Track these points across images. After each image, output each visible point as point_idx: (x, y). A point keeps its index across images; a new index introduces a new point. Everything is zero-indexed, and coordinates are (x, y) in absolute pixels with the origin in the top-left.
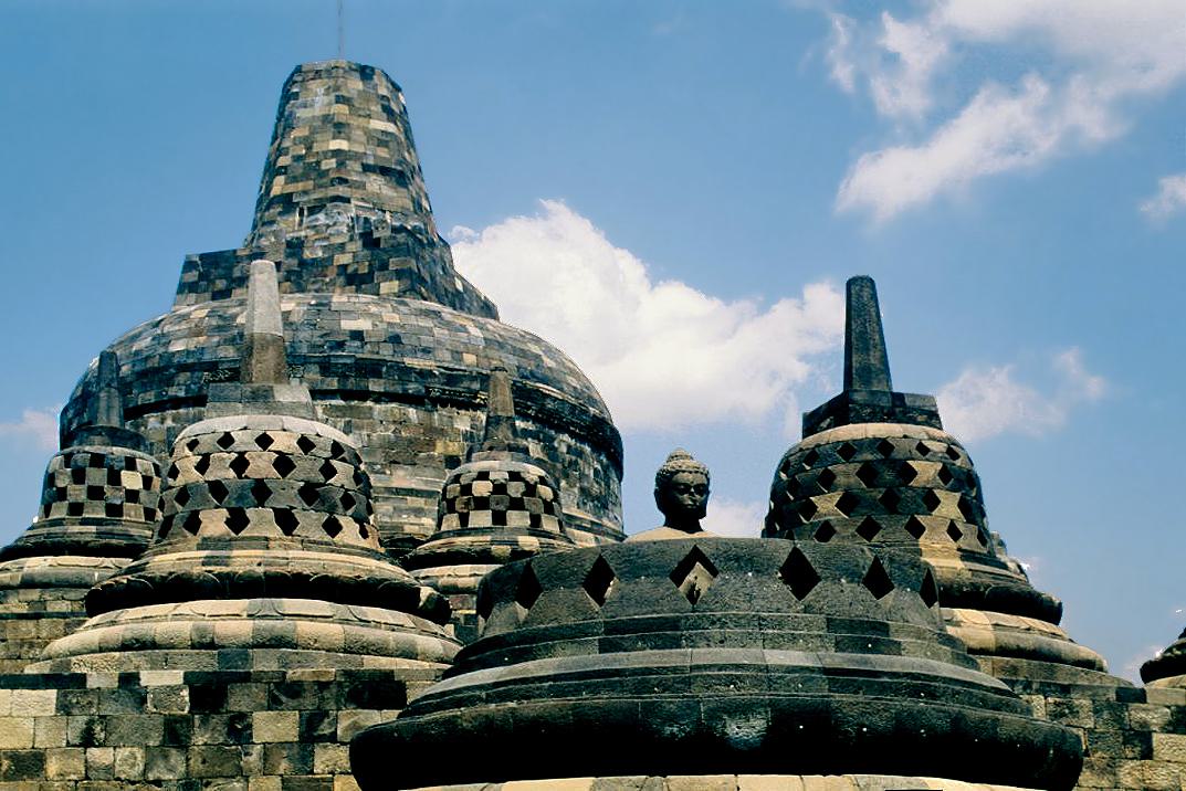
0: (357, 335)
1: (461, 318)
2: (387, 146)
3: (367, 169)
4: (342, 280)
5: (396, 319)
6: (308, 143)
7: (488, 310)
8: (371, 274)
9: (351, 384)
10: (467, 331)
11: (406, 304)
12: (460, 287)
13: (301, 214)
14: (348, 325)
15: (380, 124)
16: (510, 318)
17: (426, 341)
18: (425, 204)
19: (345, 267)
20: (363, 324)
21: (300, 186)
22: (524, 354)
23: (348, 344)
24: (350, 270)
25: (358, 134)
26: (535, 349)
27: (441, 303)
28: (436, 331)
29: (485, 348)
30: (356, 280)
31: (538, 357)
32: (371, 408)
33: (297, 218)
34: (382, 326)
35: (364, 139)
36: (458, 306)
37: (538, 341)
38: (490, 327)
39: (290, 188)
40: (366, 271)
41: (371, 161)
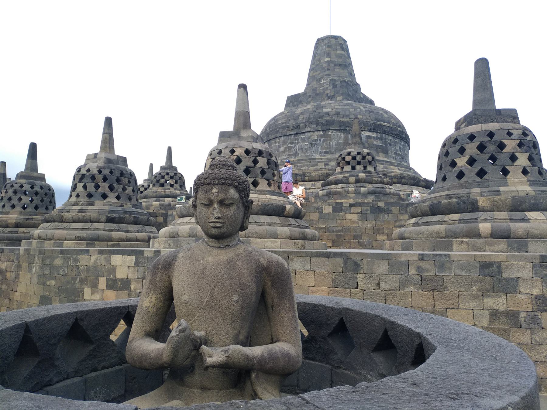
0: (328, 114)
1: (359, 105)
2: (342, 58)
3: (335, 65)
4: (326, 98)
5: (339, 107)
6: (320, 61)
7: (371, 102)
8: (334, 95)
9: (324, 128)
10: (360, 109)
11: (343, 103)
14: (325, 110)
15: (339, 52)
16: (378, 104)
17: (347, 113)
18: (353, 74)
19: (327, 94)
20: (329, 110)
21: (317, 73)
22: (378, 114)
24: (329, 95)
25: (333, 56)
26: (381, 112)
27: (355, 101)
29: (365, 113)
30: (330, 98)
31: (382, 114)
34: (334, 110)
35: (335, 57)
36: (361, 101)
37: (383, 109)
38: (367, 107)
39: (315, 74)
40: (333, 94)
41: (336, 63)
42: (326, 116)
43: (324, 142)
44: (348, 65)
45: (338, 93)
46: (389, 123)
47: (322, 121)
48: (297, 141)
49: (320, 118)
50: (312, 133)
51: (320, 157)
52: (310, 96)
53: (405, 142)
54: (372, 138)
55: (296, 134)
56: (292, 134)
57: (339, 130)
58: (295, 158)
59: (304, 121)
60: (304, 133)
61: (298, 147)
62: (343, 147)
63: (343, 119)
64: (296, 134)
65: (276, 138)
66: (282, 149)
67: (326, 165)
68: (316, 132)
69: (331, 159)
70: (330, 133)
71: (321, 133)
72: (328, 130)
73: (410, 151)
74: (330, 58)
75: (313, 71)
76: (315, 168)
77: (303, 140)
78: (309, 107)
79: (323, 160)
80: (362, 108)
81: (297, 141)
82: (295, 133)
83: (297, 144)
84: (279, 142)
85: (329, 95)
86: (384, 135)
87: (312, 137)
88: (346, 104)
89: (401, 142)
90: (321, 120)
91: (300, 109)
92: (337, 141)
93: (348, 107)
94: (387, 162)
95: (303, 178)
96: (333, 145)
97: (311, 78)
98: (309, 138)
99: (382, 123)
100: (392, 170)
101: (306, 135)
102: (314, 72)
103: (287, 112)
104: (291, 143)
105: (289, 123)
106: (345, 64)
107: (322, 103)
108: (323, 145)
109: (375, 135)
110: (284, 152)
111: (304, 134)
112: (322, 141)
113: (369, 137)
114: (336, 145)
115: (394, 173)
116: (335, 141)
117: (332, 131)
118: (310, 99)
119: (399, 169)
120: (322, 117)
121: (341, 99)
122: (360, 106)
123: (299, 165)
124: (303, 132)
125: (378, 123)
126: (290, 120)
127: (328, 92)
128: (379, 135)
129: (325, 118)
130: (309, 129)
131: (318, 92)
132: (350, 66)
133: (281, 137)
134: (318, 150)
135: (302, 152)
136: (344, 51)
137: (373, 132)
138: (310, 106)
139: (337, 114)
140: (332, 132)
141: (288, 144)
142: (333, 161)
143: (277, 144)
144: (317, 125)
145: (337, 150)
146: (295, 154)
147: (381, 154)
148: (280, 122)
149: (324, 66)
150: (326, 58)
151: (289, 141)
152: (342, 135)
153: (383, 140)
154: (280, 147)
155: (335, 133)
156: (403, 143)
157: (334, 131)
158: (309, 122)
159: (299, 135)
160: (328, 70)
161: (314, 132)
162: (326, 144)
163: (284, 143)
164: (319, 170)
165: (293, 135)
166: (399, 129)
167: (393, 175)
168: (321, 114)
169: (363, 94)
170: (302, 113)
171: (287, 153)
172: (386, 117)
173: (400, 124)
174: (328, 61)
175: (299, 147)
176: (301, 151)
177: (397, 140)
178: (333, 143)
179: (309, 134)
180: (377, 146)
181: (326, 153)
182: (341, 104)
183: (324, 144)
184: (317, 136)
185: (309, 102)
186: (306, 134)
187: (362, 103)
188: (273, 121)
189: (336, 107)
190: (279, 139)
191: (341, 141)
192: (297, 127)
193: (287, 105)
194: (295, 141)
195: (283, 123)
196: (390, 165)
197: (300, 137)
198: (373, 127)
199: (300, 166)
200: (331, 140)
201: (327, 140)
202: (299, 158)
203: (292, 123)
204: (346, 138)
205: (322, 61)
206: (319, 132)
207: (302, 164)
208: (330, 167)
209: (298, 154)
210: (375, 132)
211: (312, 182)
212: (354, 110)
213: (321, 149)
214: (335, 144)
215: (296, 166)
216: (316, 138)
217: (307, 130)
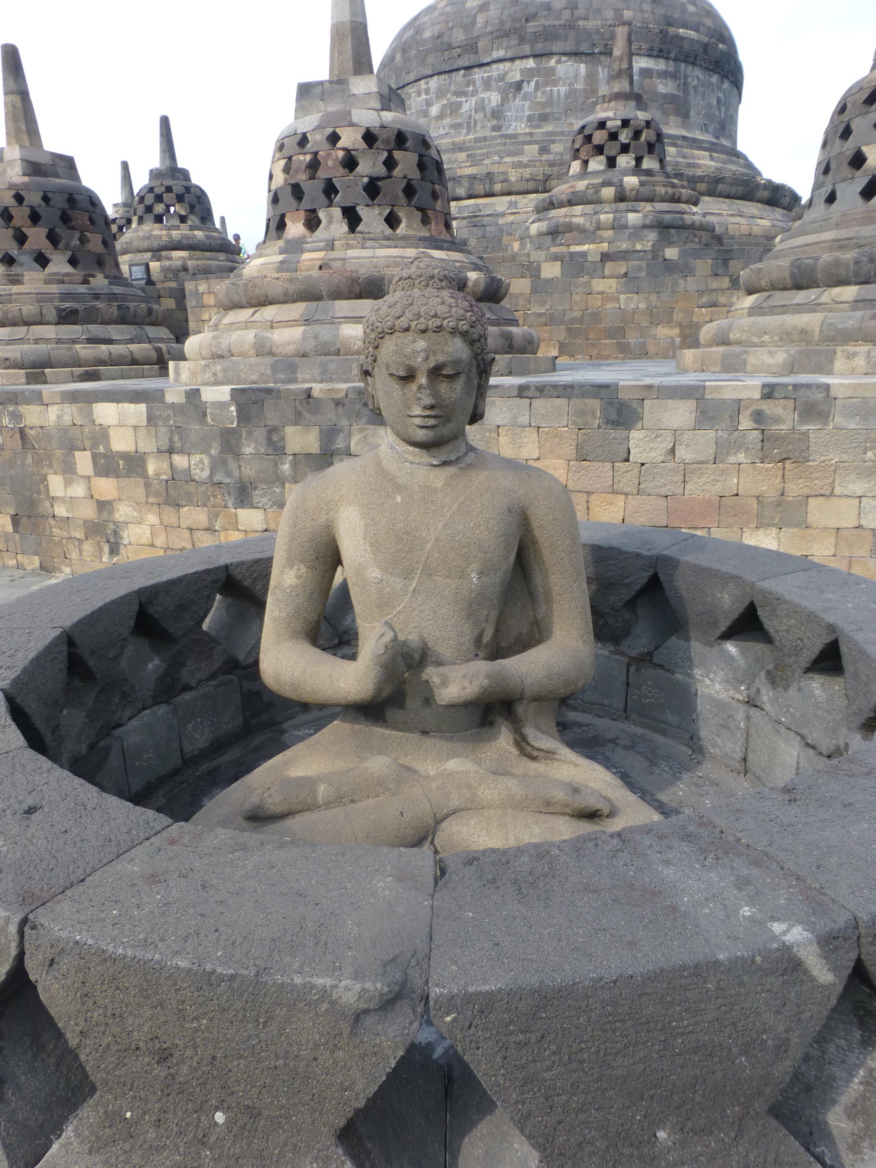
9: (540, 47)
23: (539, 14)
32: (553, 69)
42: (545, 13)
43: (537, 88)
46: (697, 30)
47: (534, 30)
48: (471, 88)
49: (527, 20)
50: (507, 65)
51: (527, 130)
53: (732, 82)
54: (655, 75)
58: (468, 133)
59: (488, 29)
60: (488, 64)
61: (473, 103)
62: (584, 102)
65: (420, 80)
66: (434, 110)
67: (544, 150)
68: (518, 62)
69: (552, 134)
73: (741, 107)
76: (516, 159)
77: (487, 84)
79: (536, 138)
81: (471, 88)
83: (473, 95)
84: (427, 91)
86: (683, 65)
87: (510, 74)
89: (722, 82)
90: (532, 27)
94: (684, 138)
95: (487, 186)
96: (559, 96)
98: (501, 78)
99: (681, 30)
100: (697, 161)
101: (496, 70)
104: (457, 94)
105: (450, 37)
109: (660, 65)
110: (440, 117)
111: (487, 68)
112: (532, 84)
113: (646, 73)
114: (568, 95)
115: (700, 168)
116: (564, 85)
119: (712, 158)
123: (478, 152)
124: (485, 61)
125: (671, 30)
126: (452, 28)
128: (671, 66)
129: (542, 21)
134: (523, 110)
135: (485, 117)
137: (658, 57)
141: (449, 95)
142: (560, 141)
143: (423, 97)
144: (522, 40)
145: (569, 110)
146: (468, 124)
147: (672, 118)
151: (453, 88)
152: (583, 67)
153: (680, 79)
154: (429, 103)
156: (726, 85)
157: (564, 58)
158: (501, 34)
159: (476, 70)
162: (543, 93)
163: (441, 93)
164: (526, 166)
165: (462, 72)
166: (721, 46)
167: (699, 172)
168: (532, 10)
171: (447, 121)
172: (692, 14)
173: (725, 33)
175: (476, 103)
176: (482, 115)
177: (715, 79)
179: (501, 66)
180: (665, 96)
181: (544, 118)
183: (539, 94)
186: (494, 66)
188: (410, 33)
190: (427, 83)
191: (580, 86)
192: (471, 47)
194: (468, 86)
196: (692, 148)
197: (478, 75)
198: (657, 44)
199: (481, 154)
200: (555, 83)
201: (546, 84)
202: (479, 135)
203: (459, 37)
204: (591, 78)
206: (525, 61)
207: (485, 150)
208: (551, 157)
209: (476, 122)
210: (662, 57)
211: (508, 198)
213: (530, 109)
215: (471, 155)
217: (496, 55)
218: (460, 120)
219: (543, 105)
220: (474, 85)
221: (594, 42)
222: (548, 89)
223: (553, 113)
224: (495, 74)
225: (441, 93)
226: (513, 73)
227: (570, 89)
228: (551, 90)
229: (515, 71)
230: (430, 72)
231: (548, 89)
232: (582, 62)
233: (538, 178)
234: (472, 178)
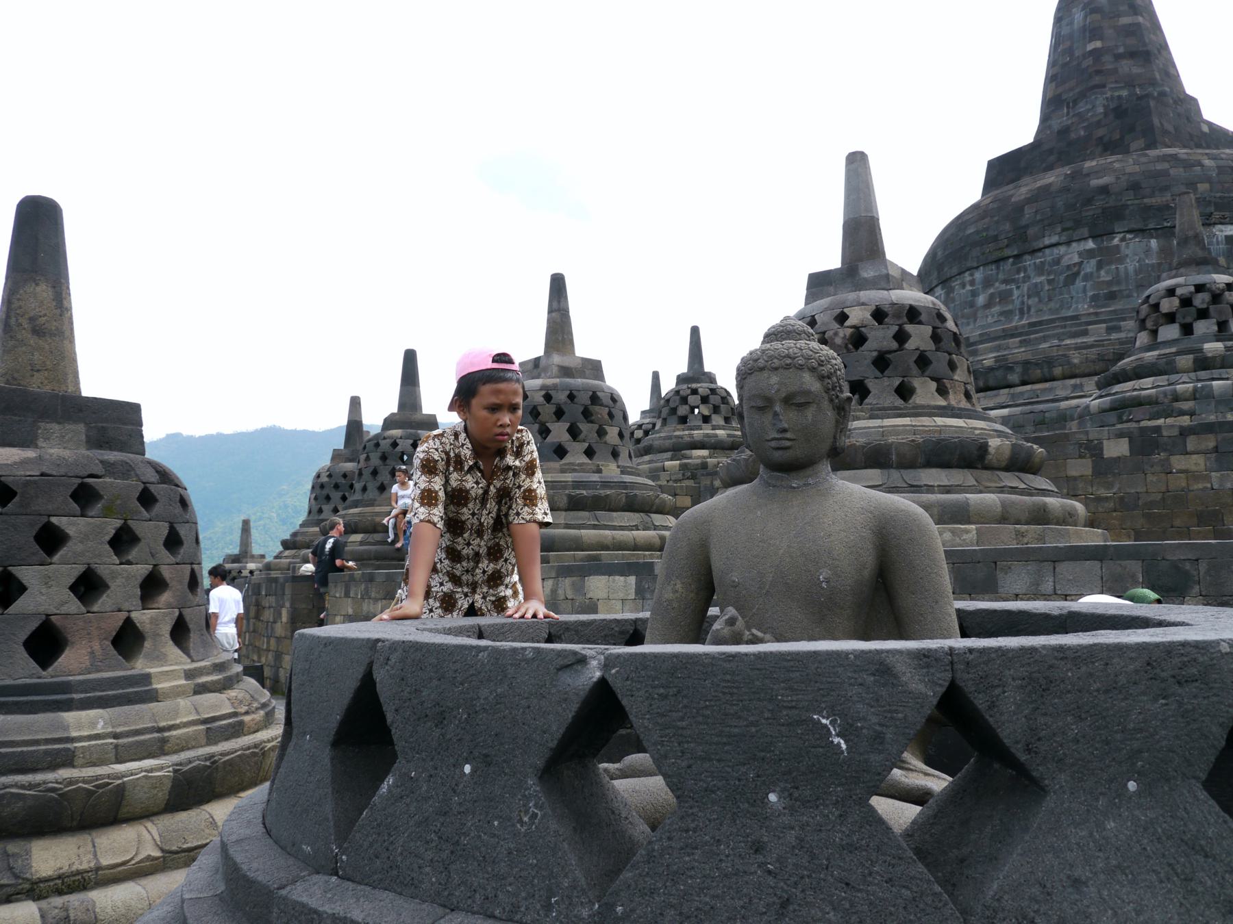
0: (1104, 190)
1: (1198, 154)
3: (1118, 57)
4: (1100, 149)
5: (1137, 169)
8: (1122, 138)
10: (1202, 166)
11: (1146, 155)
12: (1205, 129)
13: (1068, 107)
14: (1095, 182)
15: (1125, 20)
18: (1172, 71)
19: (1101, 138)
25: (1109, 32)
28: (1172, 172)
33: (1065, 111)
36: (1204, 145)
38: (1223, 156)
40: (1118, 137)
44: (1156, 52)
45: (1132, 129)
48: (1022, 275)
50: (1063, 249)
51: (1092, 310)
52: (1050, 151)
55: (1017, 257)
56: (1008, 258)
57: (1142, 231)
58: (1021, 319)
60: (1040, 250)
61: (1026, 289)
63: (1153, 200)
64: (1017, 257)
65: (964, 272)
66: (981, 300)
67: (1110, 330)
68: (1074, 245)
69: (1122, 311)
70: (1116, 241)
71: (1090, 244)
72: (1111, 233)
74: (1101, 39)
75: (1054, 84)
76: (1079, 340)
77: (1040, 269)
78: (1052, 179)
79: (1102, 317)
80: (1207, 162)
81: (1022, 275)
82: (1015, 253)
83: (1024, 282)
84: (972, 283)
85: (1106, 139)
87: (1066, 258)
88: (1158, 156)
91: (1024, 190)
92: (1138, 262)
93: (1166, 166)
95: (1046, 370)
97: (1052, 104)
101: (1049, 255)
102: (1057, 87)
103: (988, 201)
104: (1006, 282)
106: (1145, 49)
107: (1089, 164)
108: (1099, 277)
110: (988, 305)
111: (1040, 254)
114: (1137, 272)
117: (1122, 235)
118: (1052, 158)
120: (1089, 201)
121: (1143, 146)
122: (1200, 157)
123: (1032, 336)
127: (1100, 132)
130: (1055, 239)
131: (1073, 136)
132: (1164, 53)
133: (977, 268)
136: (1142, 16)
138: (1051, 178)
139: (1135, 187)
140: (1123, 240)
141: (997, 284)
143: (969, 288)
148: (971, 230)
149: (1085, 64)
150: (1090, 41)
151: (1001, 276)
152: (1154, 243)
154: (974, 294)
155: (1130, 239)
157: (1129, 236)
159: (1027, 257)
160: (1098, 72)
161: (1068, 243)
164: (1092, 346)
165: (1011, 260)
169: (1210, 124)
170: (1034, 198)
174: (1095, 50)
175: (1029, 289)
176: (1036, 299)
178: (1131, 266)
179: (1055, 250)
181: (1112, 296)
182: (1143, 160)
183: (1102, 273)
184: (1080, 254)
185: (1050, 168)
186: (1047, 251)
187: (1208, 147)
189: (1128, 170)
190: (972, 275)
193: (990, 184)
194: (1018, 272)
195: (977, 232)
197: (1028, 261)
201: (1110, 263)
204: (1165, 252)
205: (1077, 53)
206: (1083, 243)
207: (1041, 334)
208: (1123, 335)
209: (1029, 308)
211: (1073, 381)
212: (1181, 170)
214: (1135, 271)
216: (1076, 259)
217: (1047, 241)
218: (1010, 307)
219: (1109, 283)
220: (1025, 271)
221: (1165, 217)
222: (1114, 267)
223: (1120, 291)
224: (1049, 259)
225: (987, 283)
226: (1069, 256)
227: (1140, 265)
228: (1117, 268)
229: (1071, 254)
230: (975, 264)
231: (1114, 267)
232: (1152, 237)
233: (1106, 358)
234: (1026, 363)
